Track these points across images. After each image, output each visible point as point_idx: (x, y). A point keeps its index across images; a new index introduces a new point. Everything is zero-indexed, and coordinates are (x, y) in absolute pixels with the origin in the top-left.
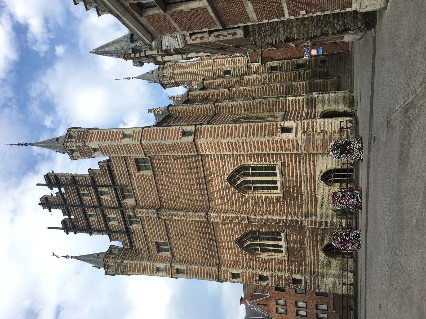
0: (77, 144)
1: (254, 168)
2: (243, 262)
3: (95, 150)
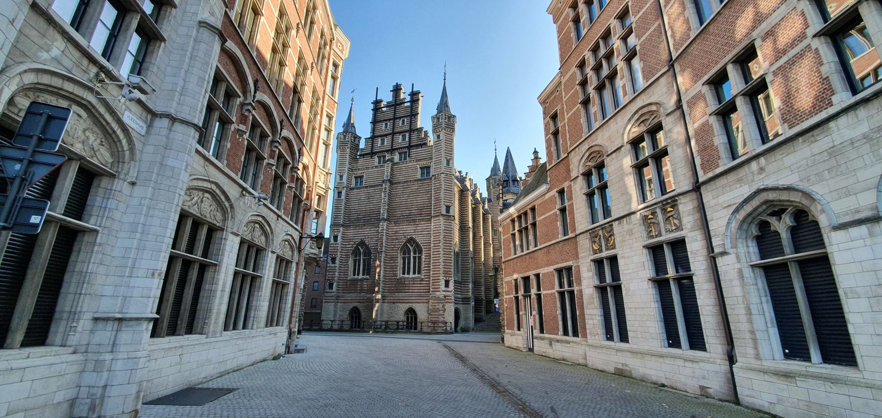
0: (444, 123)
1: (420, 258)
2: (347, 245)
3: (438, 137)
